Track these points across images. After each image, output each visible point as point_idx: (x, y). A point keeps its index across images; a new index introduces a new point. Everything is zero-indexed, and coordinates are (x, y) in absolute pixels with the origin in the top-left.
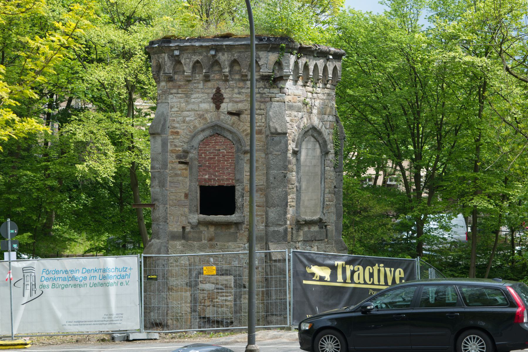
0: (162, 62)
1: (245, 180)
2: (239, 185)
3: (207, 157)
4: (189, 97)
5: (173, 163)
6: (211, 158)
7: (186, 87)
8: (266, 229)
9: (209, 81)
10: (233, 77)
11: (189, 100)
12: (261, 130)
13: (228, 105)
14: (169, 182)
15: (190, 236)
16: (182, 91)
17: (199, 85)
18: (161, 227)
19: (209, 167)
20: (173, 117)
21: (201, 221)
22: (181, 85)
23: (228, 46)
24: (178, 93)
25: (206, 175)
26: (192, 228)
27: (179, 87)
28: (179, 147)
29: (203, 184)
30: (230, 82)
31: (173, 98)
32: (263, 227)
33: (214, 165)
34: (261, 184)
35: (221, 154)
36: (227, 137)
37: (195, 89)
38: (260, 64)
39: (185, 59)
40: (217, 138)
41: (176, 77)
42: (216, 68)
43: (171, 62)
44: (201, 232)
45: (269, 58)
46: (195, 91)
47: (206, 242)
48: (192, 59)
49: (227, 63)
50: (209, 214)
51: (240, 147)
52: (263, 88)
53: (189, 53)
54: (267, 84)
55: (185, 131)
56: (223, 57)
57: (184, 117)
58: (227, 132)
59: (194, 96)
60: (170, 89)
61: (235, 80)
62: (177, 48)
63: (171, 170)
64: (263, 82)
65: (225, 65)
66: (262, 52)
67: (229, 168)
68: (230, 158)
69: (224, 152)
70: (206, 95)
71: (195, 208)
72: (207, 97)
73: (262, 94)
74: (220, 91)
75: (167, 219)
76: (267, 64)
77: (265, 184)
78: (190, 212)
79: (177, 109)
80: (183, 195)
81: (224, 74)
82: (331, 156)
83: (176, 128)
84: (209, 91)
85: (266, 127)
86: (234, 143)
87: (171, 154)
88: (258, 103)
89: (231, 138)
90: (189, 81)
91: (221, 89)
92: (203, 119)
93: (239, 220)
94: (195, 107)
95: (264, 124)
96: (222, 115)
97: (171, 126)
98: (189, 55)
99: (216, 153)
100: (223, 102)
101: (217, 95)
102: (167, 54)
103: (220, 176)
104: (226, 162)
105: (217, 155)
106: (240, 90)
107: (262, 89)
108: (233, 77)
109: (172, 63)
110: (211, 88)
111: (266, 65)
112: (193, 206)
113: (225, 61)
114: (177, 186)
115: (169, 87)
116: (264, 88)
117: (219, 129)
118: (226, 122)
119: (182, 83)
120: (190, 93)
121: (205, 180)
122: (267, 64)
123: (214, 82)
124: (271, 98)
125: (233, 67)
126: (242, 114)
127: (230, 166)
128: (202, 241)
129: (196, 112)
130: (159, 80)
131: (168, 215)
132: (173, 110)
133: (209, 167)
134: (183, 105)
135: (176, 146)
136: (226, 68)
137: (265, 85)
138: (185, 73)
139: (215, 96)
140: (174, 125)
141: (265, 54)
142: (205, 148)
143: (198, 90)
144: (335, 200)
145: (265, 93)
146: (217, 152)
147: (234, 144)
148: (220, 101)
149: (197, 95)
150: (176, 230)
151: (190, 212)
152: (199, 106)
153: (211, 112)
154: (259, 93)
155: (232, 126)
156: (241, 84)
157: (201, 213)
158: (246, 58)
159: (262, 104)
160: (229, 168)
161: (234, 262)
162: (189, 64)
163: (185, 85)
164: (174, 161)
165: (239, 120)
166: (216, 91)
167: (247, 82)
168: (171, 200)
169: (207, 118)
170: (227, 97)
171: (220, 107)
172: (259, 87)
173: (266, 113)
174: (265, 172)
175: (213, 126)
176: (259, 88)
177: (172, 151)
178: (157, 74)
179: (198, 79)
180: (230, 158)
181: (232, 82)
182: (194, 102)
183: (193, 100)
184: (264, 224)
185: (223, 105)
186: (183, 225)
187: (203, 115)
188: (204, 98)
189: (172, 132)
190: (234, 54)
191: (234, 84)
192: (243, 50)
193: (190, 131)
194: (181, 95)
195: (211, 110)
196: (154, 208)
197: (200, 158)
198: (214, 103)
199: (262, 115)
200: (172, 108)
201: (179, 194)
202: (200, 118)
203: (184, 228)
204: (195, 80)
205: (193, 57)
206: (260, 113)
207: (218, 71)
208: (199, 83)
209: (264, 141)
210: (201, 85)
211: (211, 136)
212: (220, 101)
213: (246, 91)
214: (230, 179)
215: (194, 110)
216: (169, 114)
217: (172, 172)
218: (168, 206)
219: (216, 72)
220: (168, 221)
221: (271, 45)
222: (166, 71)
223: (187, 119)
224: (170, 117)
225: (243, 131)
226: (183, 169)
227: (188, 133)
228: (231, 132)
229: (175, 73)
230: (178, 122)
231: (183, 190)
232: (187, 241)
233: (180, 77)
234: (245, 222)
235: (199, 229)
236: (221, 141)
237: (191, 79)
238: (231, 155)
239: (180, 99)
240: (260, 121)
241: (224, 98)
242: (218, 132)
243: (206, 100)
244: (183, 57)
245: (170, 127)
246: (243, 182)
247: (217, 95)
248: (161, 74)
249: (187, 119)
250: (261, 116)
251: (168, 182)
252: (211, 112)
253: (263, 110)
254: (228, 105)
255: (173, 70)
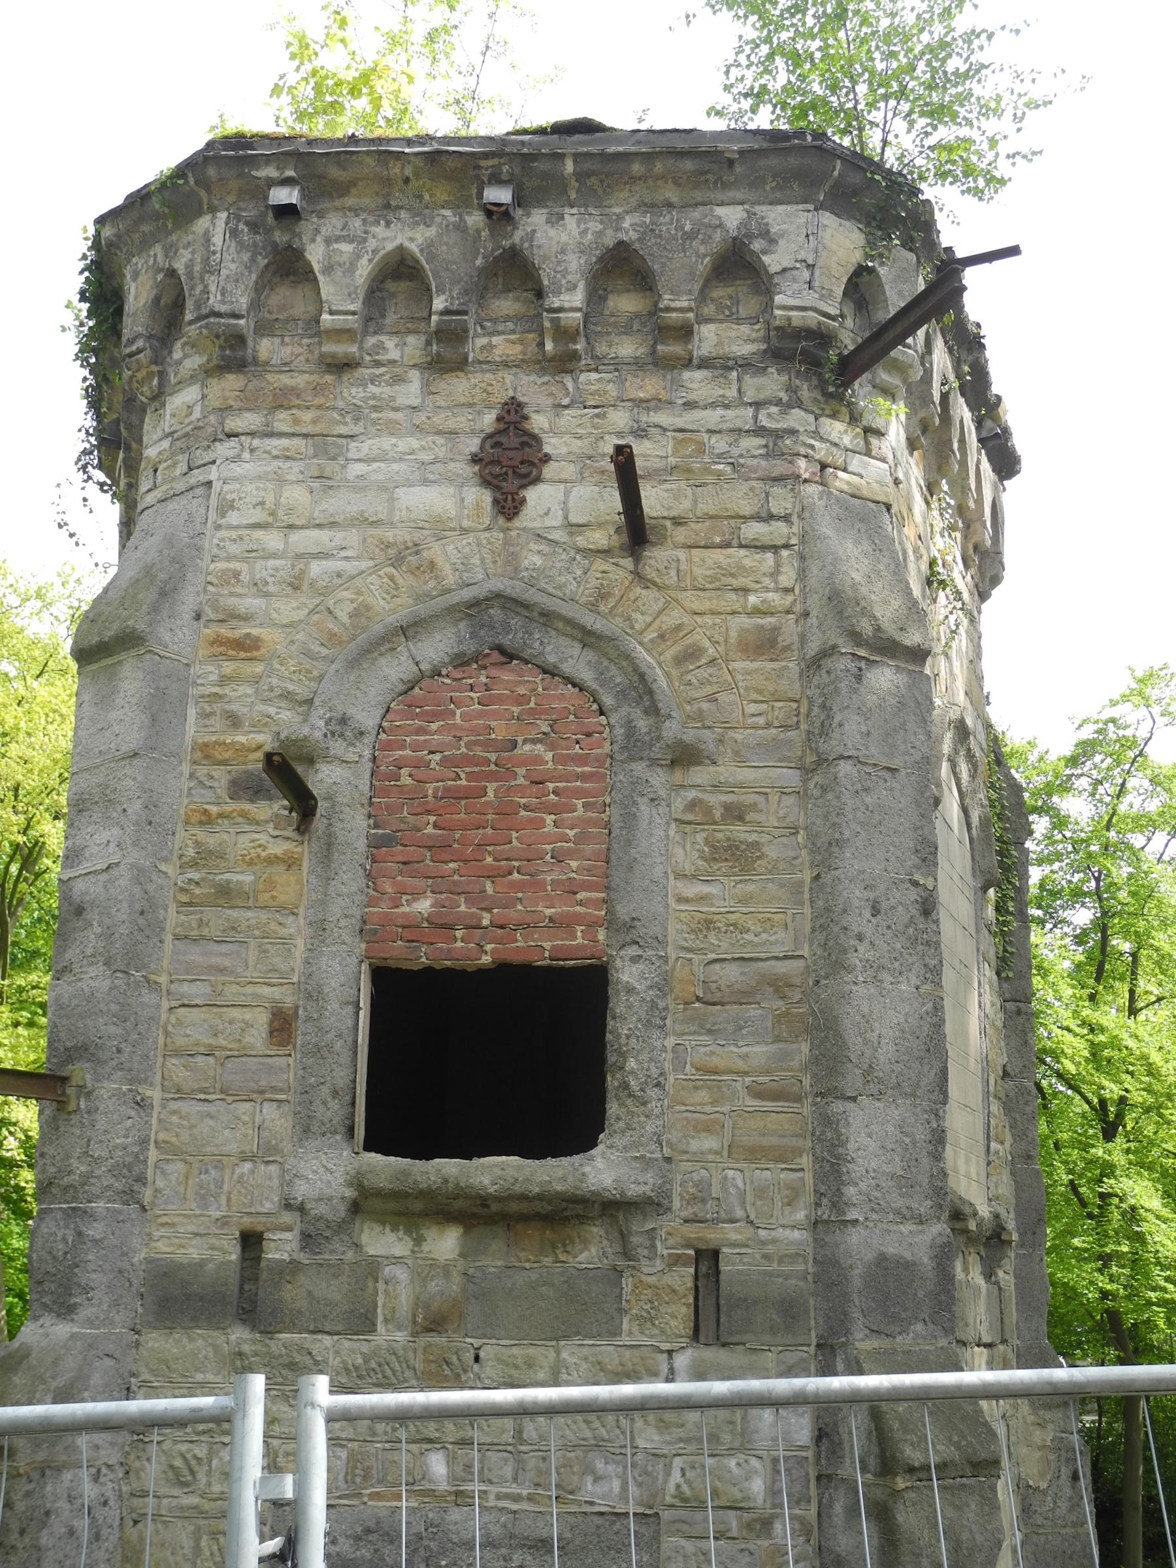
0: (189, 266)
1: (672, 927)
2: (635, 959)
3: (430, 789)
4: (333, 451)
5: (207, 820)
6: (456, 795)
7: (317, 401)
8: (819, 1243)
9: (461, 365)
10: (601, 349)
11: (330, 467)
12: (776, 630)
13: (567, 494)
14: (177, 938)
15: (293, 1294)
16: (296, 421)
17: (400, 389)
18: (95, 1231)
19: (439, 848)
20: (229, 559)
21: (379, 1194)
22: (293, 389)
23: (587, 165)
24: (272, 435)
25: (416, 895)
26: (308, 1240)
27: (282, 400)
28: (256, 727)
29: (398, 952)
30: (583, 377)
31: (237, 459)
32: (797, 1235)
33: (477, 835)
34: (778, 951)
35: (521, 771)
36: (567, 668)
37: (375, 408)
38: (773, 269)
39: (328, 241)
40: (493, 672)
41: (265, 347)
42: (506, 305)
43: (246, 256)
44: (372, 1269)
45: (826, 236)
46: (374, 423)
47: (401, 1337)
48: (372, 244)
49: (575, 264)
50: (428, 1156)
51: (642, 724)
52: (779, 402)
53: (356, 211)
54: (805, 387)
55: (300, 637)
56: (552, 233)
57: (299, 556)
58: (563, 641)
59: (366, 447)
60: (225, 410)
61: (617, 365)
62: (290, 173)
63: (194, 864)
64: (779, 372)
65: (566, 272)
66: (781, 208)
67: (570, 854)
68: (579, 793)
69: (538, 760)
70: (440, 440)
71: (334, 1105)
72: (441, 453)
73: (777, 435)
74: (526, 418)
75: (141, 1180)
76: (811, 267)
77: (805, 952)
78: (305, 1130)
79: (259, 516)
80: (262, 1019)
81: (556, 322)
82: (990, 912)
83: (246, 618)
84: (461, 421)
85: (806, 614)
86: (608, 700)
87: (202, 771)
88: (754, 483)
89: (586, 676)
90: (342, 367)
91: (526, 411)
92: (416, 571)
93: (639, 1185)
94: (375, 506)
95: (790, 598)
96: (534, 547)
97: (216, 610)
98: (357, 223)
99: (488, 762)
100: (537, 480)
101: (503, 439)
102: (223, 216)
103: (509, 904)
104: (550, 819)
105: (492, 777)
106: (644, 418)
107: (774, 410)
108: (601, 349)
109: (253, 260)
110: (470, 405)
111: (806, 275)
112: (325, 1091)
113: (563, 251)
114: (227, 962)
115: (217, 404)
116: (785, 407)
117: (516, 622)
118: (560, 587)
119: (300, 380)
120: (343, 430)
121: (410, 924)
122: (811, 267)
123: (489, 376)
124: (824, 466)
125: (604, 299)
126: (654, 544)
127: (582, 838)
128: (372, 1330)
129: (372, 531)
130: (161, 385)
131: (153, 1154)
132: (233, 518)
133: (439, 848)
134: (296, 495)
135: (235, 721)
136: (572, 288)
137: (791, 389)
138: (325, 317)
139: (497, 444)
140: (232, 601)
141: (803, 218)
142: (421, 731)
143: (392, 415)
144: (1009, 1140)
145: (793, 432)
146: (493, 757)
147: (602, 713)
148: (523, 470)
149: (387, 442)
150: (194, 1252)
151: (305, 1130)
152: (392, 500)
153: (465, 531)
154: (759, 431)
155: (593, 607)
156: (650, 385)
157: (368, 1147)
158: (691, 236)
159: (777, 490)
160: (570, 854)
161: (597, 1479)
162: (351, 269)
163: (317, 390)
164: (214, 809)
165: (637, 574)
166: (499, 419)
167: (687, 375)
168: (177, 1053)
169: (440, 561)
170: (564, 450)
171: (523, 501)
172: (761, 397)
173: (803, 538)
174: (807, 876)
175: (475, 603)
176: (757, 405)
177: (206, 753)
178: (155, 351)
179: (392, 362)
180: (579, 793)
181: (594, 376)
182: (361, 477)
183: (357, 469)
184: (801, 1215)
185: (539, 498)
186: (247, 1222)
187: (417, 548)
188: (426, 457)
189: (217, 641)
190: (620, 217)
191: (610, 387)
192: (671, 194)
193: (332, 635)
194: (285, 442)
195: (466, 523)
196: (61, 1105)
197: (385, 792)
198: (486, 482)
199: (775, 549)
200: (226, 506)
201: (235, 1013)
202: (398, 561)
203: (251, 1241)
204: (378, 364)
205: (374, 229)
206: (767, 540)
207: (517, 318)
208: (398, 380)
209: (796, 690)
210: (411, 391)
211: (461, 661)
212: (523, 470)
213: (680, 422)
214: (577, 919)
215: (362, 521)
216: (211, 541)
217: (196, 876)
218: (155, 1094)
219: (501, 327)
220: (147, 1195)
221: (838, 164)
222: (215, 301)
223: (316, 569)
224: (214, 559)
225: (662, 637)
226: (272, 860)
227: (316, 648)
228: (588, 638)
229: (264, 329)
230: (259, 588)
231: (267, 990)
232: (269, 1333)
233: (288, 350)
234: (676, 1204)
235: (358, 1246)
236: (522, 690)
237: (353, 349)
238: (584, 777)
239: (277, 463)
240: (767, 581)
241: (547, 459)
242: (506, 641)
243: (439, 467)
244: (317, 231)
245: (209, 613)
246: (661, 942)
247: (503, 439)
248: (177, 355)
249: (316, 569)
250: (769, 556)
251: (169, 938)
252: (465, 531)
253: (786, 518)
254: (567, 494)
255: (256, 305)
